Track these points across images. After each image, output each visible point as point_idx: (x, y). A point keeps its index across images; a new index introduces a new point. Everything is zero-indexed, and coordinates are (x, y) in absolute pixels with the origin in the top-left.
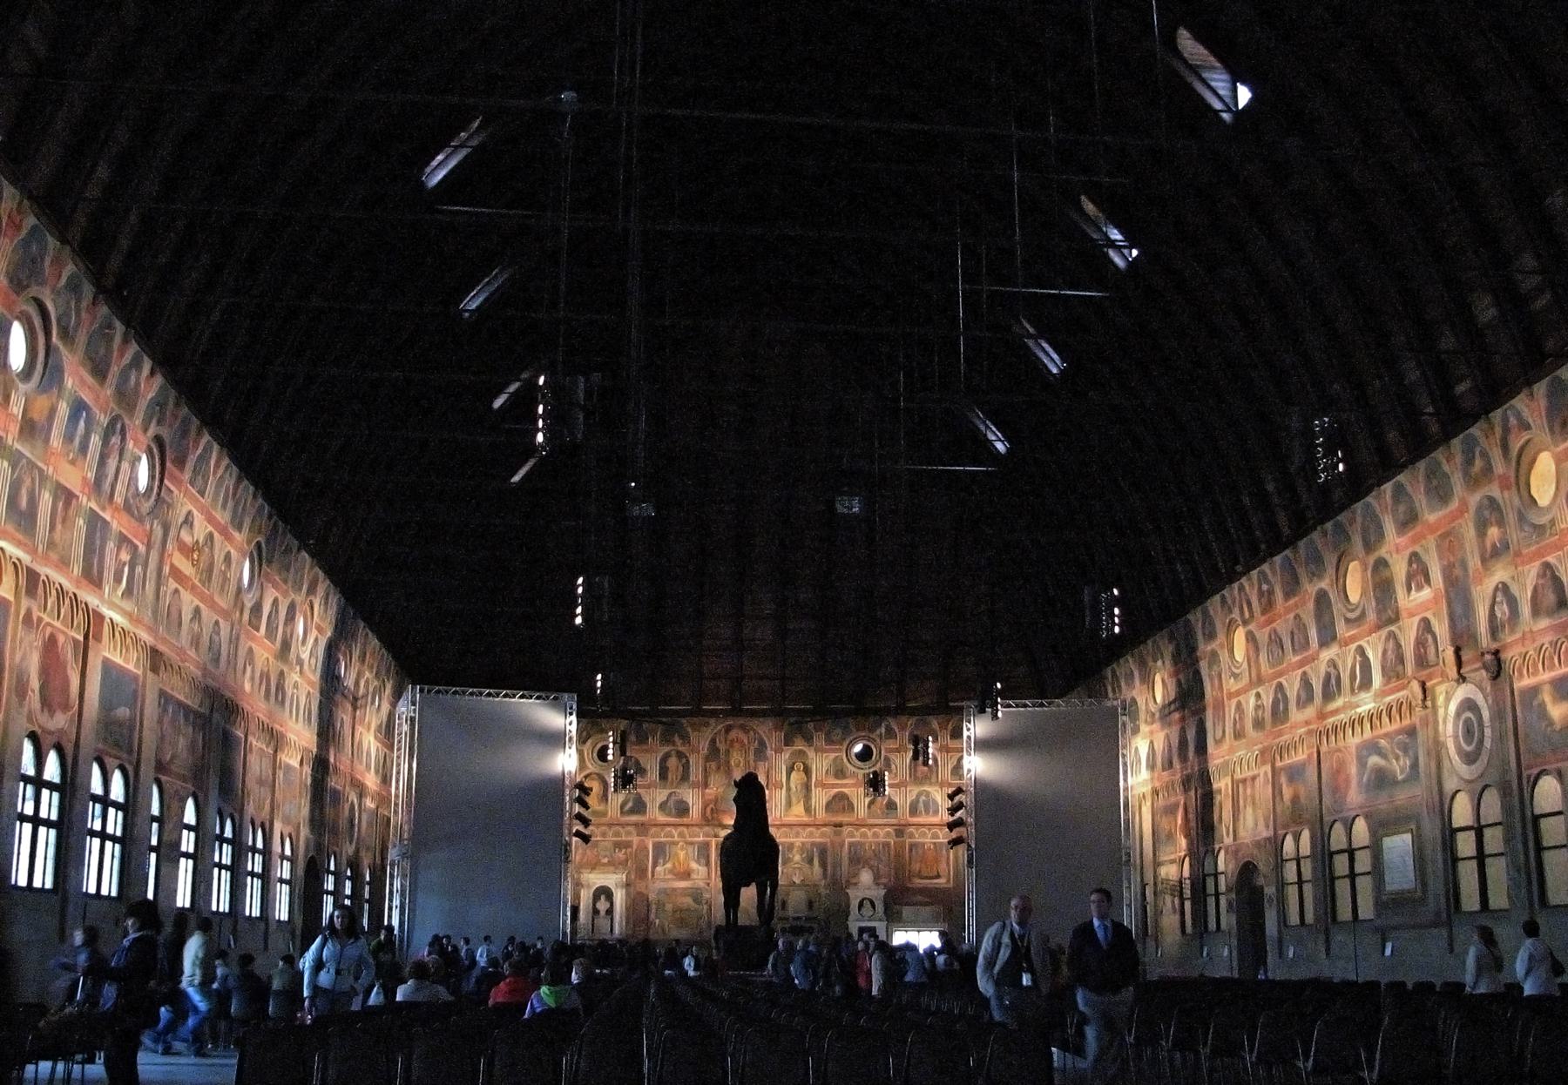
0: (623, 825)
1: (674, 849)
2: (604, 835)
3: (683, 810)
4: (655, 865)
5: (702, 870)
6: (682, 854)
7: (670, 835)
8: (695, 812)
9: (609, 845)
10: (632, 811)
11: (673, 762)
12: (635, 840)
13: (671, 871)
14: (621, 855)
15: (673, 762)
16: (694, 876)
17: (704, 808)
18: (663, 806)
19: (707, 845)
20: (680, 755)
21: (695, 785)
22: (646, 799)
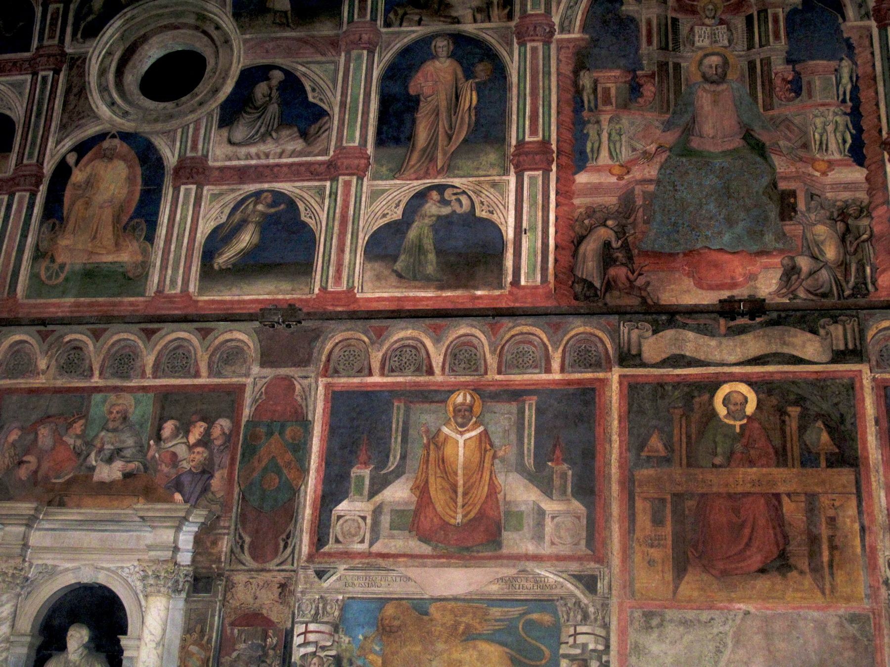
0: (200, 319)
1: (426, 417)
2: (123, 362)
3: (472, 251)
4: (334, 490)
5: (561, 511)
6: (461, 443)
7: (414, 359)
8: (529, 262)
9: (140, 409)
10: (251, 267)
11: (437, 76)
12: (254, 378)
13: (413, 521)
14: (183, 449)
15: (437, 76)
16: (517, 541)
17: (571, 242)
18: (385, 246)
19: (587, 397)
20: (471, 52)
21: (527, 158)
22: (317, 213)
